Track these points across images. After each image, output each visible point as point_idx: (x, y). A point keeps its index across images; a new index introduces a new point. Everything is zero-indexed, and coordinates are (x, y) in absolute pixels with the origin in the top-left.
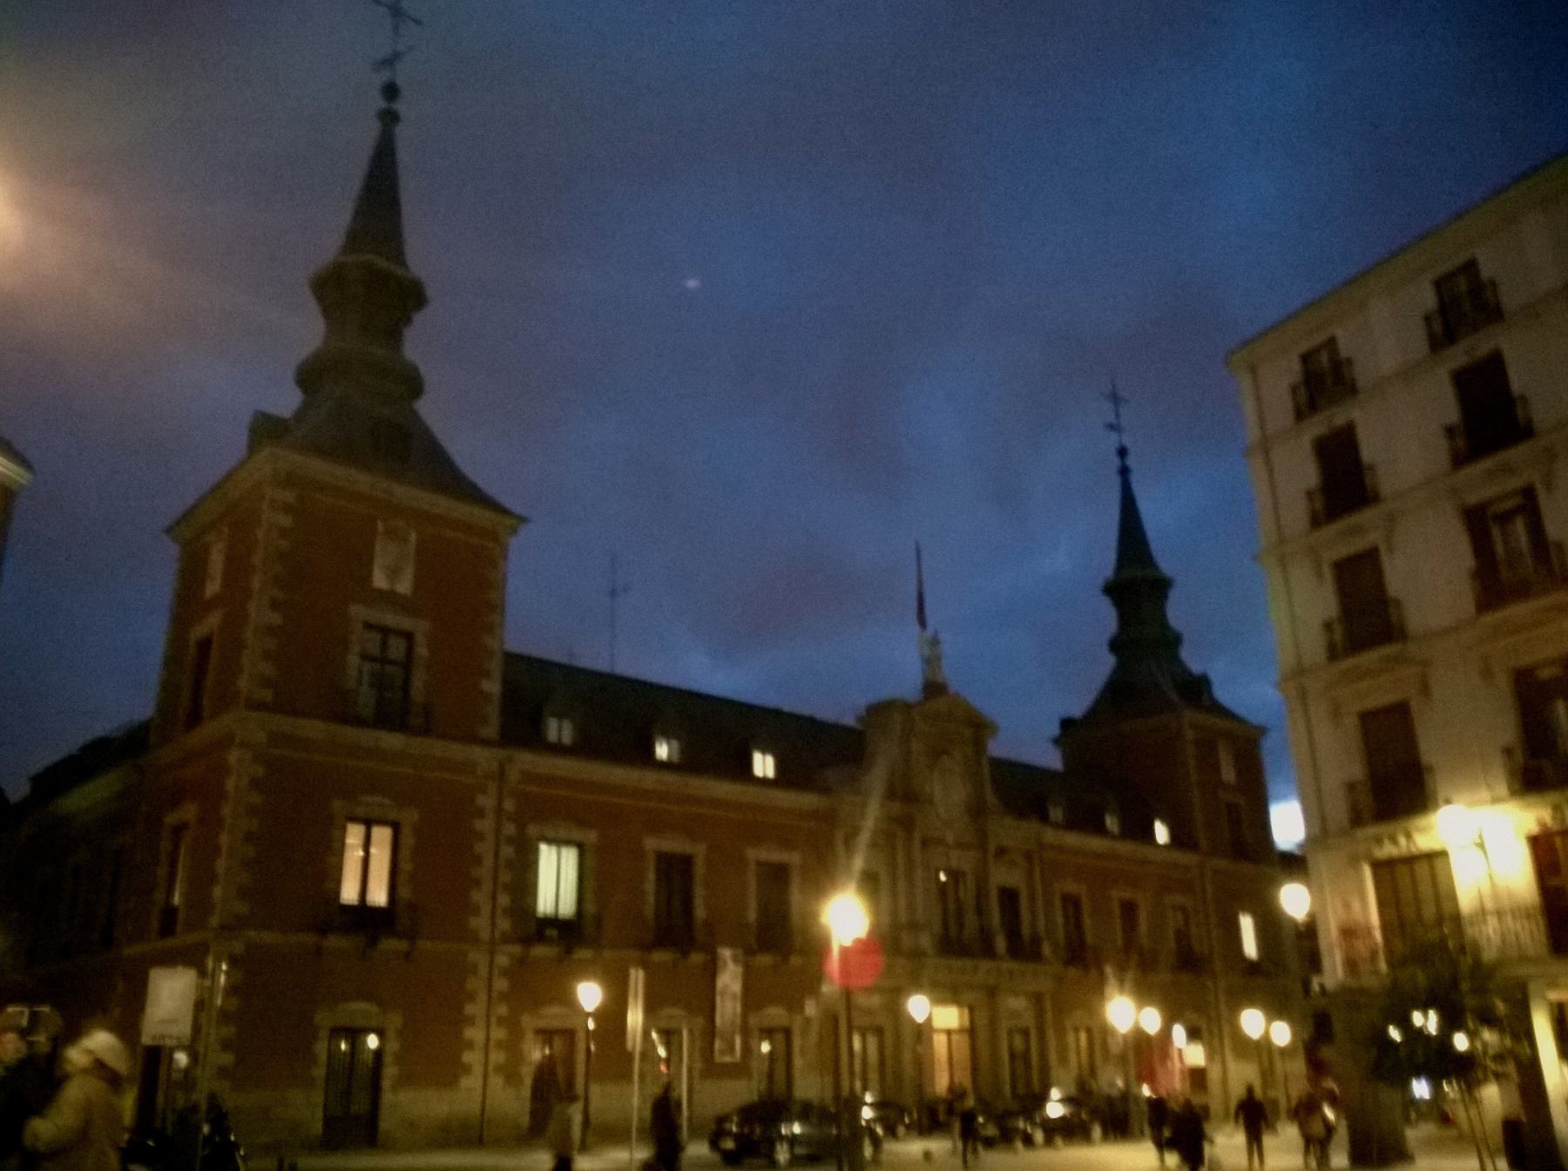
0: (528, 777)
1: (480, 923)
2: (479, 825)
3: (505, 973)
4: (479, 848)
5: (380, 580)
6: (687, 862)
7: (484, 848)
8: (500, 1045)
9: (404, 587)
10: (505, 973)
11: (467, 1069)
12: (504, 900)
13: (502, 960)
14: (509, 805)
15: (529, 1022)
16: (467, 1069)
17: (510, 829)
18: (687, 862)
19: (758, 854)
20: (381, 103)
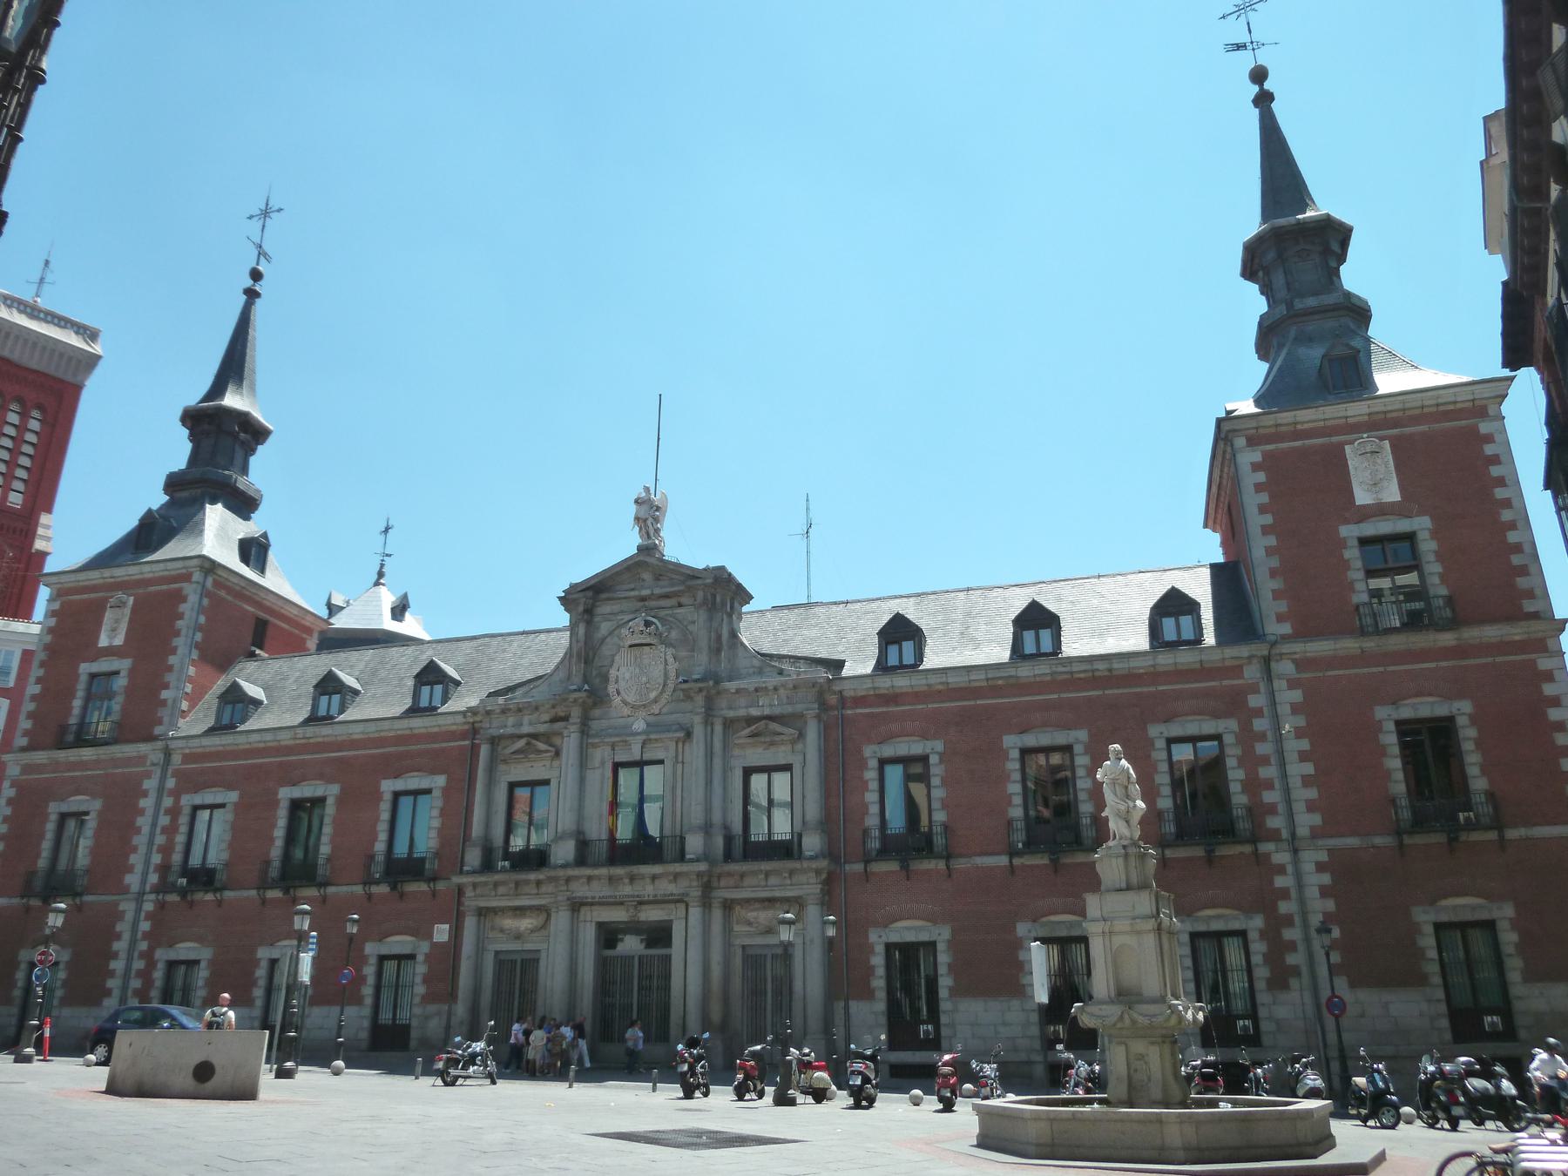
0: (187, 758)
1: (132, 880)
2: (143, 803)
3: (149, 916)
4: (140, 821)
5: (103, 641)
6: (1443, 730)
7: (143, 822)
8: (1292, 946)
9: (119, 641)
10: (149, 916)
11: (108, 993)
12: (157, 859)
13: (149, 907)
14: (171, 783)
15: (162, 955)
16: (108, 993)
17: (168, 802)
18: (1443, 730)
19: (388, 786)
20: (249, 283)
